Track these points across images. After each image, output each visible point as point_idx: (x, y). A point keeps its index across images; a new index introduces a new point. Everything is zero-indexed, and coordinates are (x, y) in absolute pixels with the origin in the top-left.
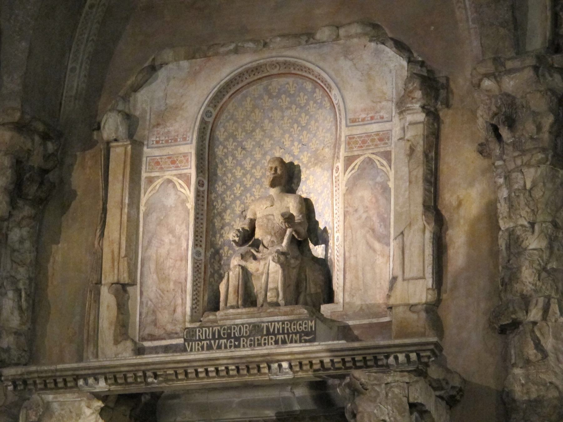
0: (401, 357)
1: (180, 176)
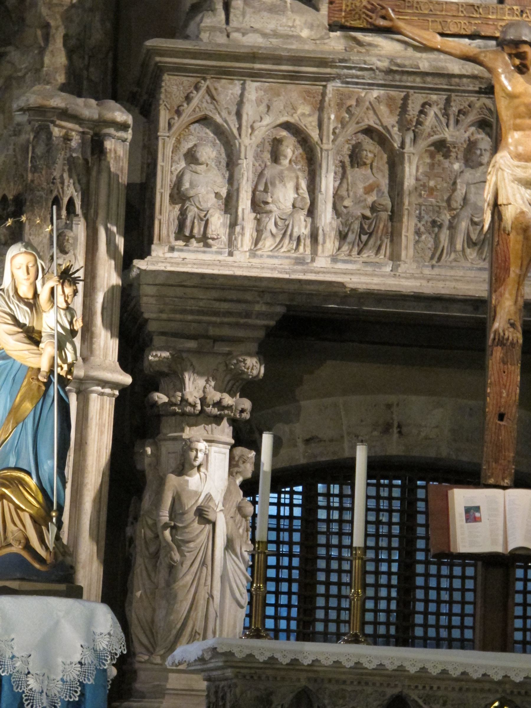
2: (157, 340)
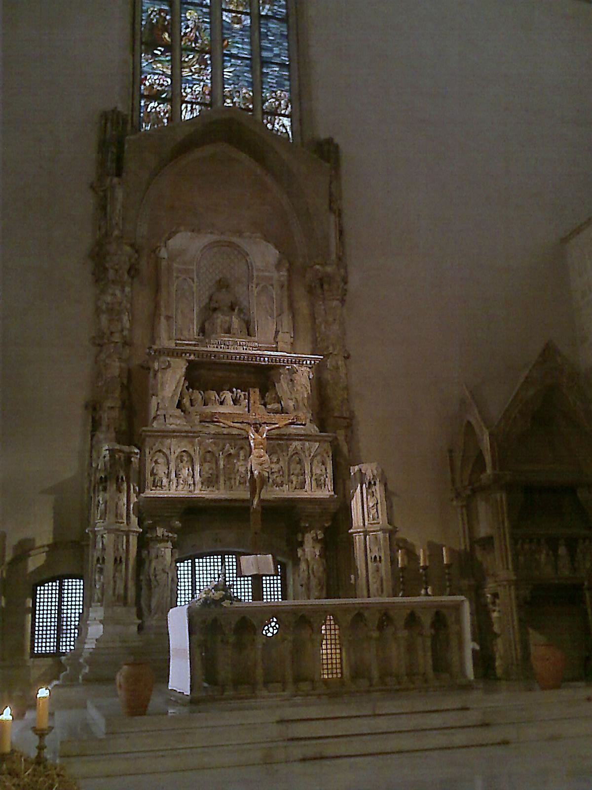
0: (308, 362)
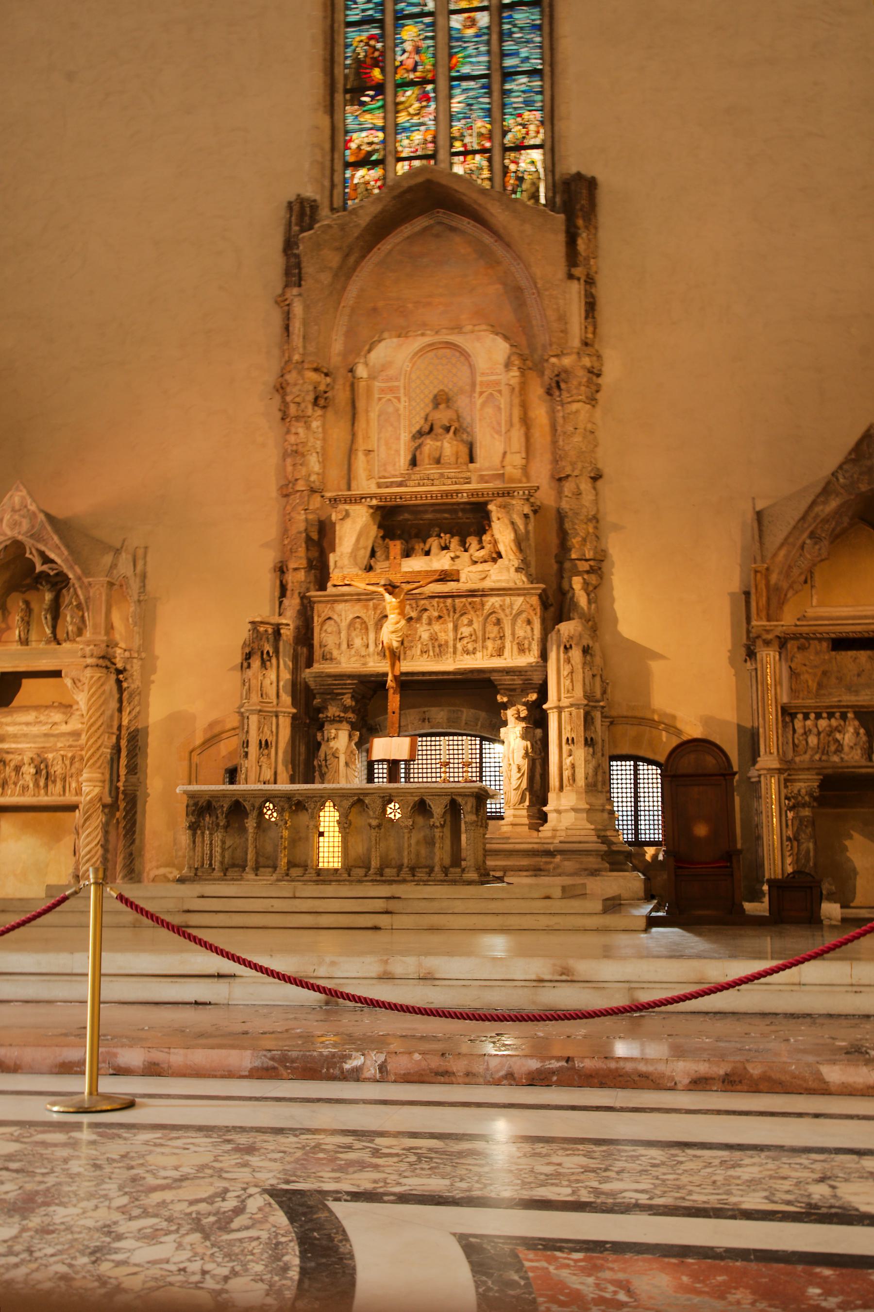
1: (395, 397)
2: (317, 696)
